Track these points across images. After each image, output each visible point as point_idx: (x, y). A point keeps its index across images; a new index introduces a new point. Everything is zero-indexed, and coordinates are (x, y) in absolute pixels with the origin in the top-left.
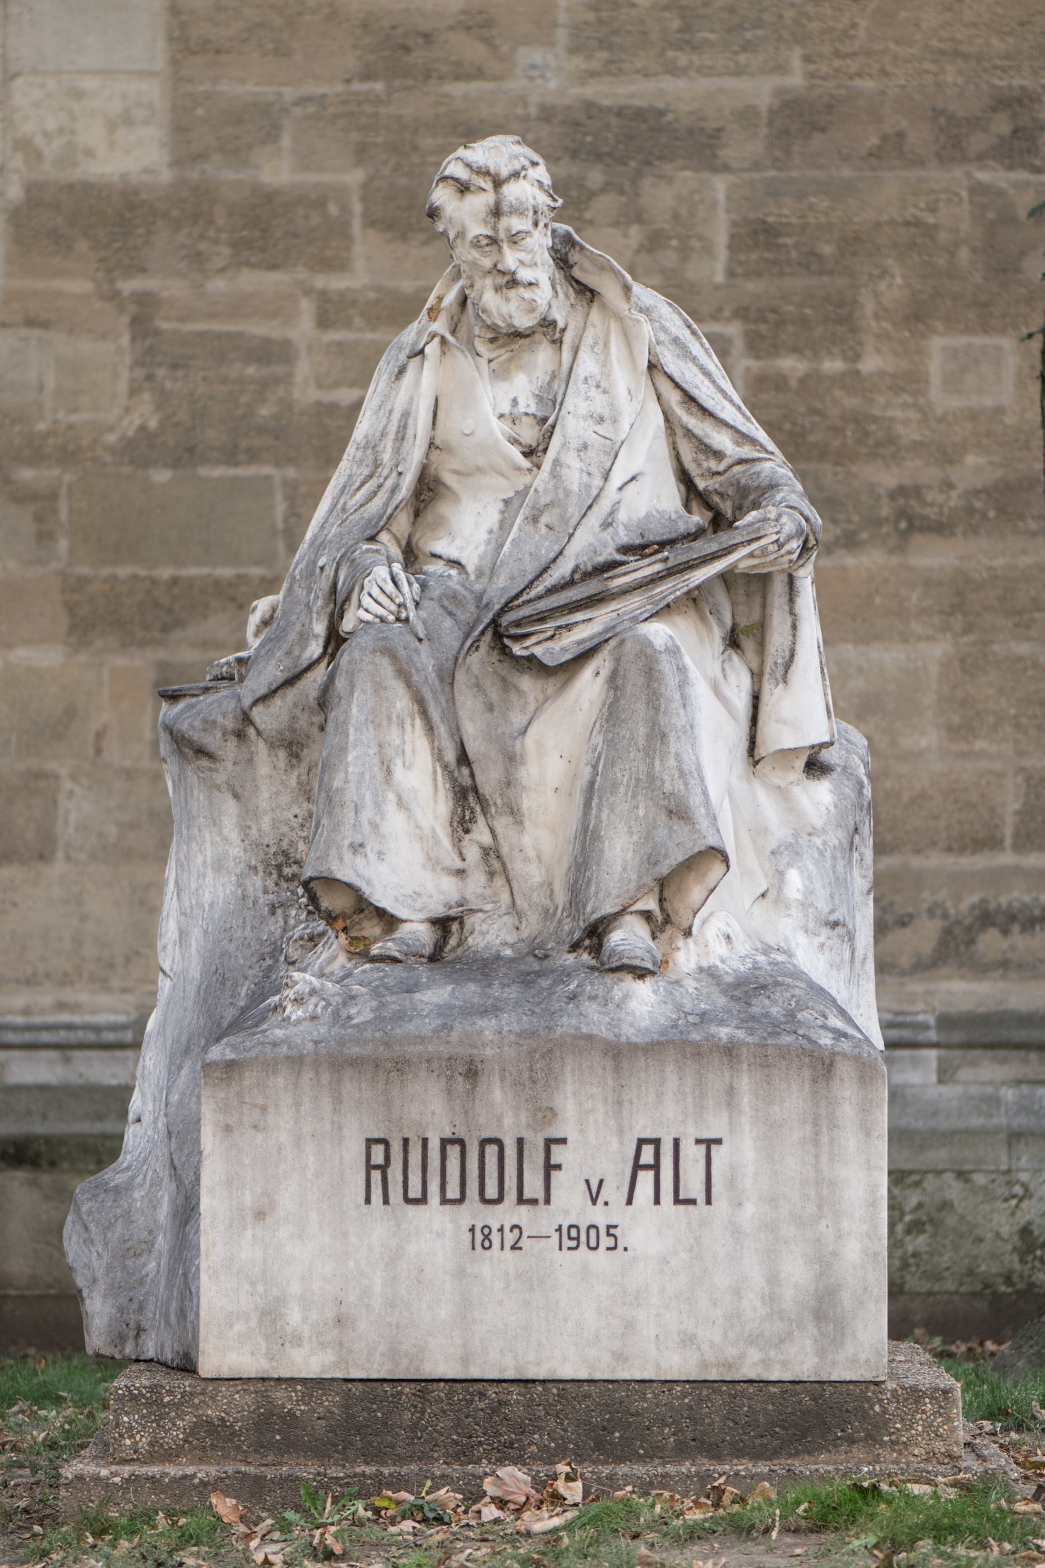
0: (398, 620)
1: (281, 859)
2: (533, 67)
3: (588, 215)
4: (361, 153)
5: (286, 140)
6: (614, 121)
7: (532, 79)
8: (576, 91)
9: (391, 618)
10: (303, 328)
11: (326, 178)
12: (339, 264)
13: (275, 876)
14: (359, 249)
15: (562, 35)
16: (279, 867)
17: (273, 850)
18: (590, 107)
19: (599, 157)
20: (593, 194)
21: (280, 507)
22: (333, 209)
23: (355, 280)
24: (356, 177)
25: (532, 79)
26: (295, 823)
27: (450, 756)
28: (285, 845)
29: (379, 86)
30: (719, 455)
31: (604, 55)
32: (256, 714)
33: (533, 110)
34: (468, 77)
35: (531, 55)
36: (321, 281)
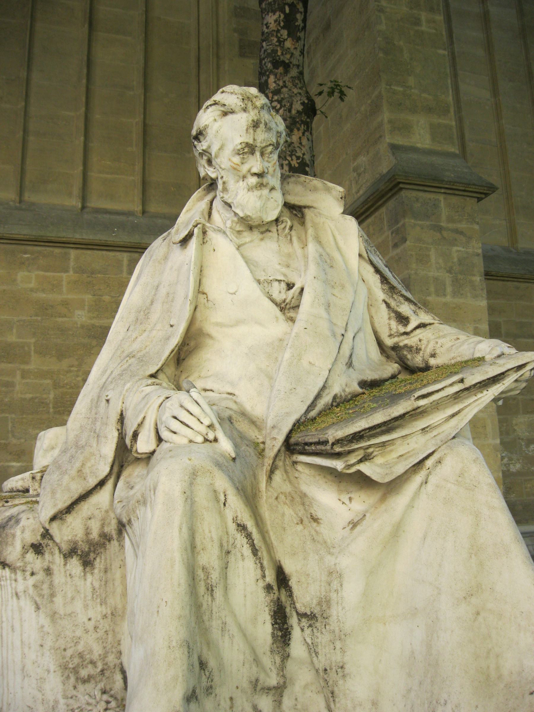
0: (206, 440)
1: (76, 660)
2: (79, 315)
3: (92, 352)
4: (34, 334)
5: (15, 331)
6: (99, 329)
7: (79, 318)
8: (89, 321)
9: (200, 439)
10: (18, 378)
11: (25, 340)
12: (27, 363)
13: (72, 679)
14: (33, 358)
15: (86, 307)
16: (75, 670)
17: (69, 652)
18: (93, 326)
19: (95, 338)
20: (93, 347)
21: (10, 425)
22: (26, 348)
23: (32, 366)
24: (33, 340)
25: (79, 318)
26: (90, 626)
27: (271, 577)
28: (80, 648)
29: (39, 318)
30: (403, 320)
31: (97, 313)
32: (55, 529)
33: (79, 326)
34: (63, 317)
35: (78, 312)
36: (22, 367)
